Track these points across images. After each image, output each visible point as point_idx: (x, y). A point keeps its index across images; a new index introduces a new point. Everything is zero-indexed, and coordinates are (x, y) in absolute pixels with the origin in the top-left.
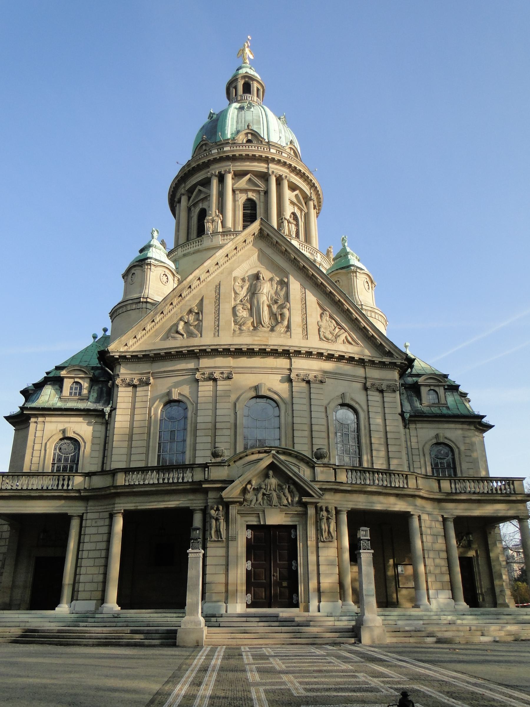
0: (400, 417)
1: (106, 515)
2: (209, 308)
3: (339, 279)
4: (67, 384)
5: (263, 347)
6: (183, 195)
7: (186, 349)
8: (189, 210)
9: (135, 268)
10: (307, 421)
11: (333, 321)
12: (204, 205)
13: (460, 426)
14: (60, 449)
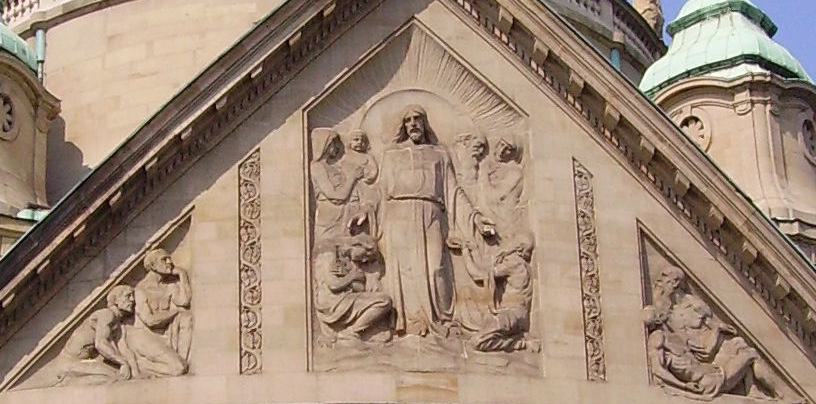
3: (696, 113)
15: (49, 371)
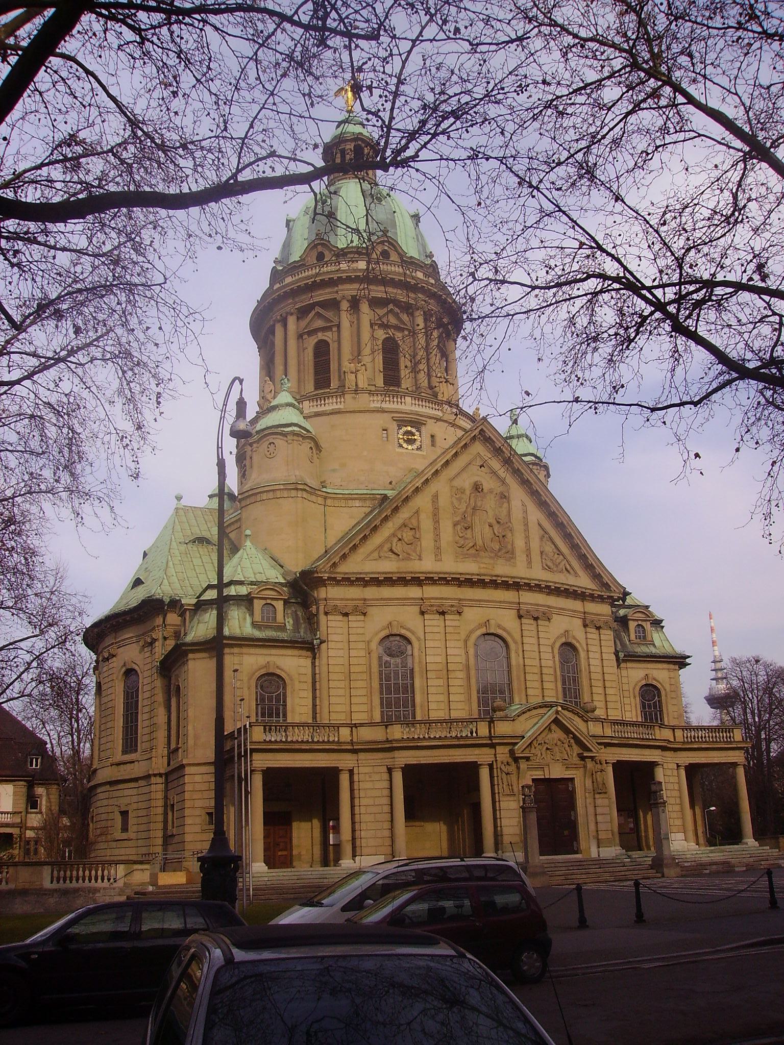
0: (614, 657)
1: (384, 769)
2: (426, 523)
4: (258, 604)
5: (494, 578)
6: (292, 314)
7: (410, 575)
8: (300, 336)
9: (274, 436)
10: (537, 663)
11: (553, 546)
12: (328, 336)
13: (665, 666)
14: (262, 687)
15: (376, 555)
